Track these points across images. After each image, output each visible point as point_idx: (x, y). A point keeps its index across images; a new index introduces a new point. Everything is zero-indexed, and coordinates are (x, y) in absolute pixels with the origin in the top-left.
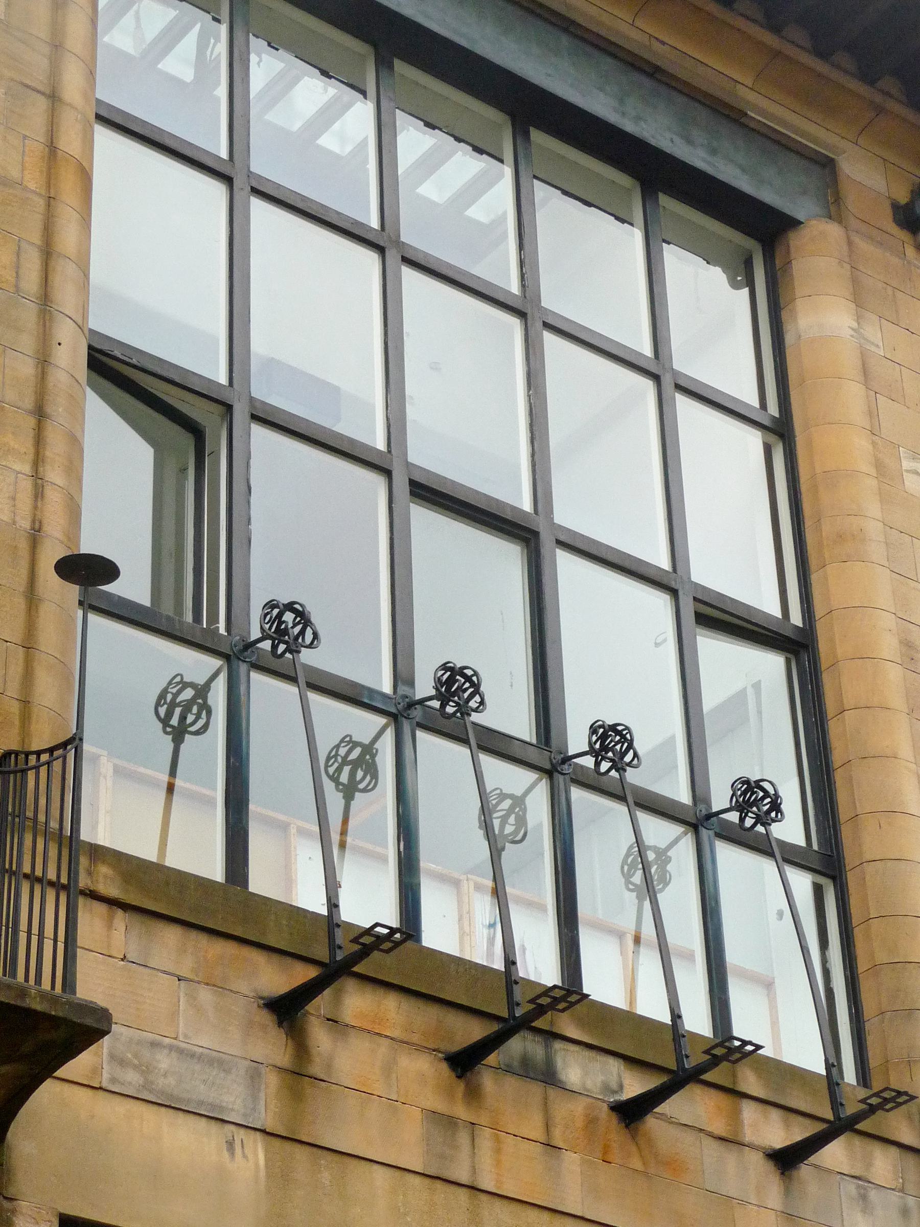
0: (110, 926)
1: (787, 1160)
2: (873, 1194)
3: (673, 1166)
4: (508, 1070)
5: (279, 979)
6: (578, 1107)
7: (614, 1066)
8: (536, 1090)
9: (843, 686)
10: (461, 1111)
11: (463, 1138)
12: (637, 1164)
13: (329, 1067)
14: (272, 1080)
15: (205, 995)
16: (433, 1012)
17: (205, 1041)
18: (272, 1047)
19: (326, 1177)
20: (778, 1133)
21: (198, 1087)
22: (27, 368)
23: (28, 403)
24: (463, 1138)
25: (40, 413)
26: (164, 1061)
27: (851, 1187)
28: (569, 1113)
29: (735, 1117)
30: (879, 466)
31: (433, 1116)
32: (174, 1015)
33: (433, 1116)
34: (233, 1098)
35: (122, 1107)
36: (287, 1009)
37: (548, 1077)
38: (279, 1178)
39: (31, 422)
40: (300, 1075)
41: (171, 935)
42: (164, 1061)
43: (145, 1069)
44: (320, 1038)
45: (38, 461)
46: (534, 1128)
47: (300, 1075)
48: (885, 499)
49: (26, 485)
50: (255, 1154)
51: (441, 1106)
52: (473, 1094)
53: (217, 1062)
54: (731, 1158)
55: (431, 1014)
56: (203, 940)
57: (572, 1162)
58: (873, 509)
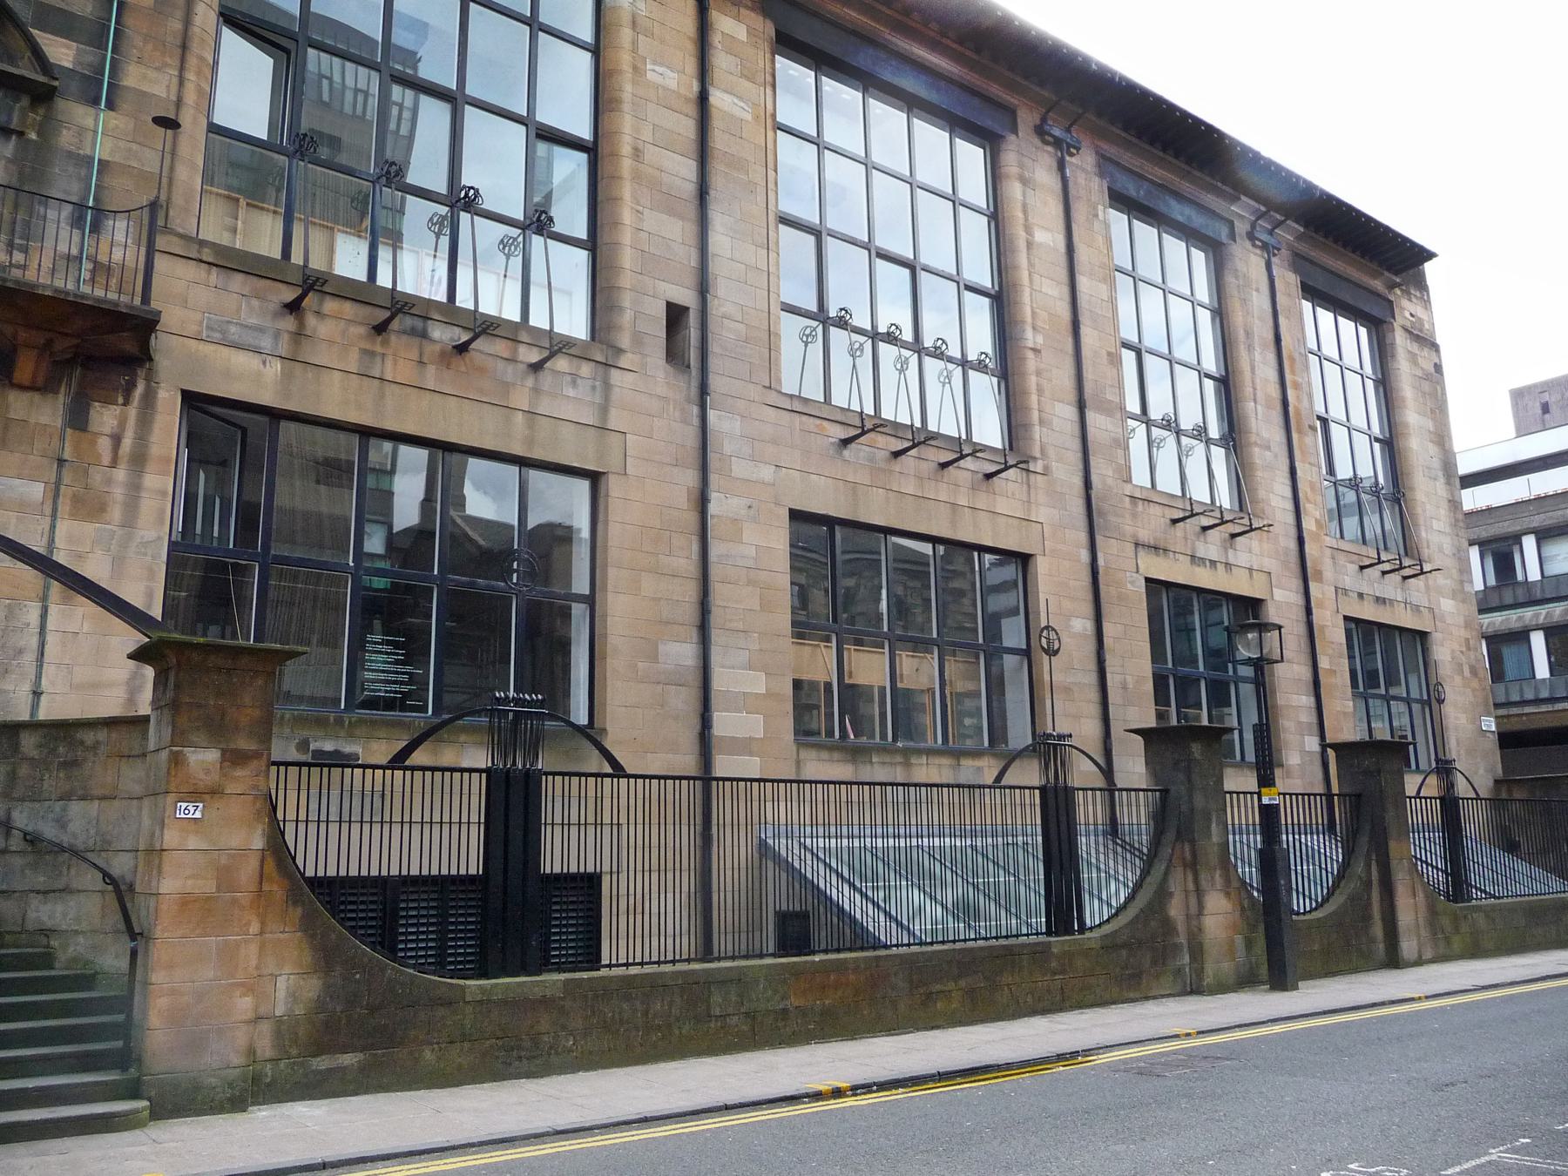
0: (209, 273)
1: (536, 367)
2: (579, 381)
3: (482, 370)
4: (404, 332)
5: (289, 295)
6: (437, 348)
7: (457, 330)
8: (417, 340)
9: (605, 168)
10: (379, 349)
11: (378, 359)
12: (463, 369)
13: (315, 330)
14: (286, 337)
15: (255, 303)
16: (369, 309)
17: (253, 321)
18: (289, 323)
19: (310, 375)
20: (534, 356)
21: (249, 338)
22: (176, 25)
23: (178, 42)
24: (378, 359)
25: (184, 47)
26: (233, 329)
27: (569, 378)
28: (430, 349)
29: (515, 351)
30: (635, 68)
31: (365, 352)
32: (239, 309)
33: (365, 352)
34: (266, 343)
35: (212, 347)
36: (294, 307)
37: (424, 335)
38: (287, 376)
39: (179, 51)
40: (299, 335)
41: (239, 277)
42: (233, 329)
43: (223, 332)
44: (311, 320)
45: (182, 69)
46: (415, 355)
47: (299, 335)
48: (634, 83)
49: (175, 81)
50: (277, 365)
51: (368, 346)
52: (385, 343)
53: (260, 330)
54: (510, 368)
55: (368, 310)
56: (255, 279)
57: (431, 370)
58: (628, 88)
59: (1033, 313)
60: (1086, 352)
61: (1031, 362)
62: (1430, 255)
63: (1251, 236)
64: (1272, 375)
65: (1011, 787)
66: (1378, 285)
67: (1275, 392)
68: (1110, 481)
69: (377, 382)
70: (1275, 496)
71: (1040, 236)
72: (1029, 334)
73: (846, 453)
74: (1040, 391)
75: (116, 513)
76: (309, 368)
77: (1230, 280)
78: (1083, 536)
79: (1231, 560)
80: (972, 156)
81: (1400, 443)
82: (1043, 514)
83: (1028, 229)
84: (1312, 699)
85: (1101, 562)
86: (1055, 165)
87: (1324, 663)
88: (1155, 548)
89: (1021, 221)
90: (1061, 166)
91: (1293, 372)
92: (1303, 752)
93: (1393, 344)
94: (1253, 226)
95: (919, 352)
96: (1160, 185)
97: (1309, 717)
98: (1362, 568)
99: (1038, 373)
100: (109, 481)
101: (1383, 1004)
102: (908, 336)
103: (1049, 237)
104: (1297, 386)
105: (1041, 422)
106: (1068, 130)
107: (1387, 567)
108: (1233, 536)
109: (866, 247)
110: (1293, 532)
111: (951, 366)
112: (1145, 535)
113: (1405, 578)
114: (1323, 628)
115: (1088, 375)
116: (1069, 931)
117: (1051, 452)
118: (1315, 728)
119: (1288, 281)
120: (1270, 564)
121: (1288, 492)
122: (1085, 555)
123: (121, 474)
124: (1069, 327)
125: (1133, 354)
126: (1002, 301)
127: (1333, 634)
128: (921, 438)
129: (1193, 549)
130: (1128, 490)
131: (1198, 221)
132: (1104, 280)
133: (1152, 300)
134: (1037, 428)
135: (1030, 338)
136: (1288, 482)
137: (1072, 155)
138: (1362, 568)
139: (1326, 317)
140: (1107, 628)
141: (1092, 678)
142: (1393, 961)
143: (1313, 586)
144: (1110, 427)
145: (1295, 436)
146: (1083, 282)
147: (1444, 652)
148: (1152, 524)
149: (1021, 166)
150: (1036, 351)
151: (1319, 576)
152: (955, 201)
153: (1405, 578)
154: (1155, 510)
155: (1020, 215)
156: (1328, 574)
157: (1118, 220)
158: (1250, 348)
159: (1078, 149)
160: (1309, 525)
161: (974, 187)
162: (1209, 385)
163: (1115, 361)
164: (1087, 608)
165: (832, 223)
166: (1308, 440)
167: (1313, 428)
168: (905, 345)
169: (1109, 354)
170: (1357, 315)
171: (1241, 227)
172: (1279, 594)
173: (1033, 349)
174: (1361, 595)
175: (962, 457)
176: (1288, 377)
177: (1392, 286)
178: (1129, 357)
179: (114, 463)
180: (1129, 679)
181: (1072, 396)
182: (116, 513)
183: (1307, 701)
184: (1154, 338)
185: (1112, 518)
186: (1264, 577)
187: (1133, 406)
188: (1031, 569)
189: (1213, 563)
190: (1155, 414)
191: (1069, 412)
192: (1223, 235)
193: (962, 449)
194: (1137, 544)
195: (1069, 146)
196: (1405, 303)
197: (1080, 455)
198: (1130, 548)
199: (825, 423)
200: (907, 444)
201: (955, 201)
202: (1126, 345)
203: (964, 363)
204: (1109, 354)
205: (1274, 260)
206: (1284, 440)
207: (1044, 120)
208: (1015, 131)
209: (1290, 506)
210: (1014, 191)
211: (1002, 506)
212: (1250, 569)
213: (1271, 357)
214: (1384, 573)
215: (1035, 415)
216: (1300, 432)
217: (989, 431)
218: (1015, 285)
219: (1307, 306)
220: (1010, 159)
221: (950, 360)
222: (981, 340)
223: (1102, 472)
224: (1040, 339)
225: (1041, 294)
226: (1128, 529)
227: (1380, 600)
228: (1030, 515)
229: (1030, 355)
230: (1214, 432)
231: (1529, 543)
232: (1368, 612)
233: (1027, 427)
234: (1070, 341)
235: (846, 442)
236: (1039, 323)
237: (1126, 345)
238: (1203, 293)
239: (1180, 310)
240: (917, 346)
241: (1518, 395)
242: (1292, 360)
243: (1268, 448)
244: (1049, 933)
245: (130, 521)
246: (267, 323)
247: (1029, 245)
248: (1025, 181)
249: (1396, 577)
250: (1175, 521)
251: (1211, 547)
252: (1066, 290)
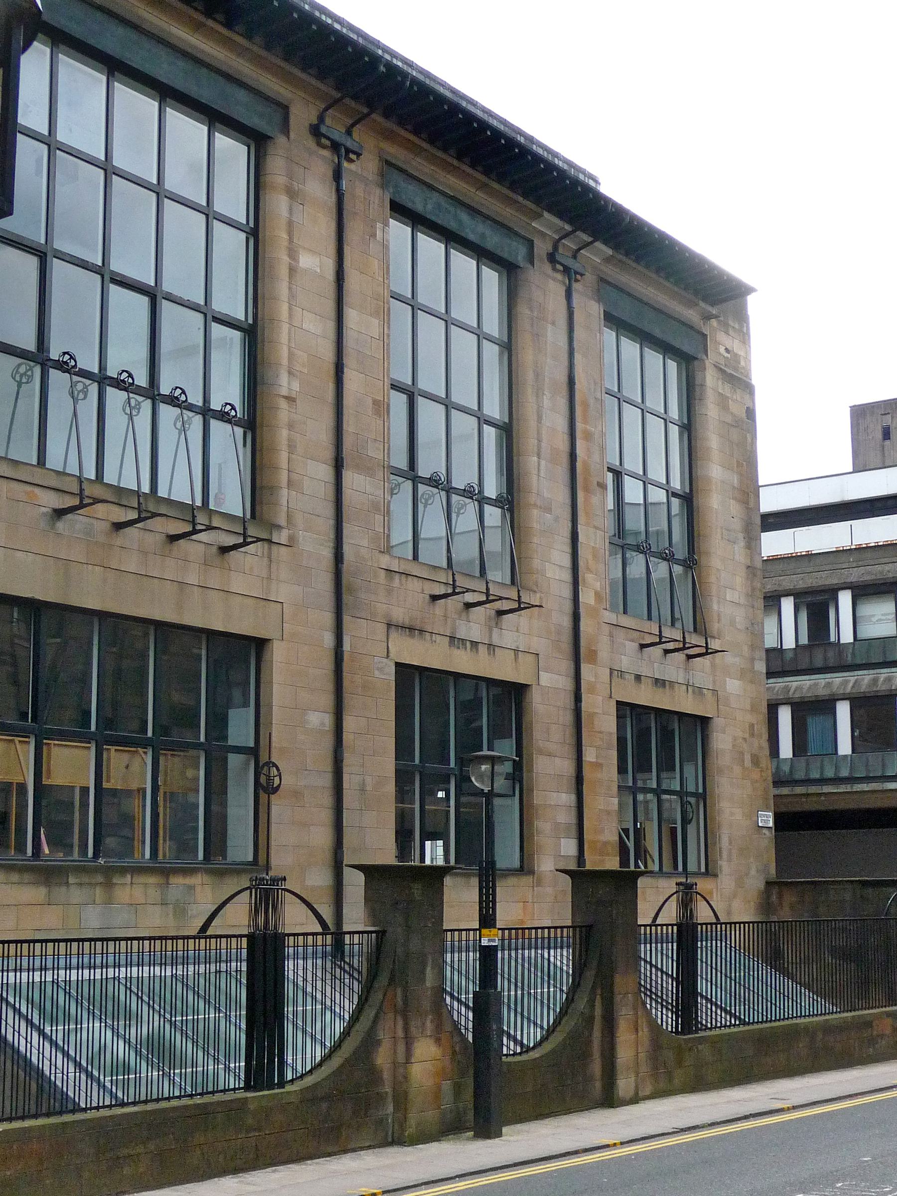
59: (291, 355)
60: (349, 400)
61: (284, 413)
62: (749, 290)
63: (552, 258)
64: (561, 423)
65: (216, 937)
66: (691, 315)
67: (562, 444)
68: (364, 552)
70: (551, 564)
71: (306, 261)
72: (284, 379)
73: (60, 525)
74: (292, 447)
77: (523, 310)
78: (328, 618)
79: (496, 641)
80: (233, 152)
81: (700, 501)
82: (284, 592)
83: (292, 254)
84: (573, 797)
85: (346, 647)
86: (330, 174)
87: (589, 755)
88: (411, 630)
89: (286, 244)
90: (337, 175)
91: (585, 421)
92: (558, 856)
93: (703, 385)
94: (555, 247)
95: (153, 399)
96: (452, 198)
97: (567, 818)
98: (643, 646)
99: (291, 426)
101: (576, 1153)
102: (142, 380)
103: (316, 263)
104: (588, 436)
105: (289, 482)
106: (349, 132)
107: (671, 646)
108: (500, 613)
109: (100, 271)
110: (568, 606)
111: (187, 414)
112: (399, 615)
113: (689, 657)
114: (592, 715)
115: (349, 426)
116: (271, 1086)
117: (299, 519)
118: (574, 831)
119: (589, 310)
120: (539, 644)
121: (567, 561)
122: (329, 639)
124: (332, 371)
125: (404, 397)
126: (253, 335)
127: (604, 723)
128: (146, 507)
129: (454, 629)
130: (385, 561)
131: (493, 240)
132: (375, 314)
133: (431, 330)
134: (285, 492)
135: (285, 383)
136: (568, 549)
137: (352, 161)
138: (643, 646)
139: (631, 348)
140: (349, 723)
141: (327, 780)
142: (609, 1100)
143: (585, 668)
144: (369, 489)
145: (580, 495)
146: (352, 316)
147: (723, 741)
148: (409, 599)
149: (290, 176)
150: (290, 399)
151: (593, 656)
152: (209, 214)
153: (689, 657)
154: (414, 585)
155: (285, 236)
156: (604, 654)
157: (399, 232)
158: (539, 392)
159: (358, 155)
160: (587, 598)
161: (233, 199)
162: (490, 433)
163: (382, 409)
164: (327, 700)
165: (60, 244)
166: (595, 500)
167: (602, 486)
168: (139, 391)
169: (375, 402)
170: (667, 349)
171: (542, 248)
172: (546, 679)
173: (286, 398)
174: (638, 678)
175: (195, 532)
176: (579, 426)
177: (707, 317)
178: (399, 401)
180: (368, 780)
181: (328, 453)
183: (569, 799)
184: (431, 380)
185: (362, 596)
186: (530, 658)
187: (402, 463)
188: (266, 657)
189: (474, 644)
190: (424, 471)
191: (324, 472)
192: (520, 257)
193: (194, 518)
194: (389, 625)
195: (348, 151)
196: (721, 336)
197: (332, 522)
198: (381, 628)
199: (37, 490)
200: (133, 515)
201: (209, 214)
202: (395, 387)
203: (206, 412)
204: (375, 402)
205: (575, 286)
206: (568, 501)
207: (321, 119)
208: (285, 129)
209: (567, 576)
210: (278, 205)
211: (238, 584)
212: (516, 651)
213: (562, 402)
214: (667, 652)
215: (284, 477)
216: (587, 490)
217: (231, 498)
218: (272, 320)
219: (610, 336)
220: (276, 165)
221: (190, 408)
222: (228, 390)
223: (356, 540)
224: (296, 386)
225: (301, 332)
226: (381, 608)
227: (659, 683)
228: (266, 596)
229: (283, 404)
230: (491, 490)
231: (845, 599)
232: (644, 696)
233: (273, 489)
234: (331, 387)
235: (59, 513)
236: (298, 367)
237: (395, 387)
238: (493, 325)
239: (464, 342)
240: (152, 392)
241: (860, 414)
242: (586, 405)
243: (548, 510)
244: (248, 1087)
247: (292, 270)
248: (292, 194)
249: (680, 657)
250: (434, 598)
251: (474, 627)
252: (331, 326)
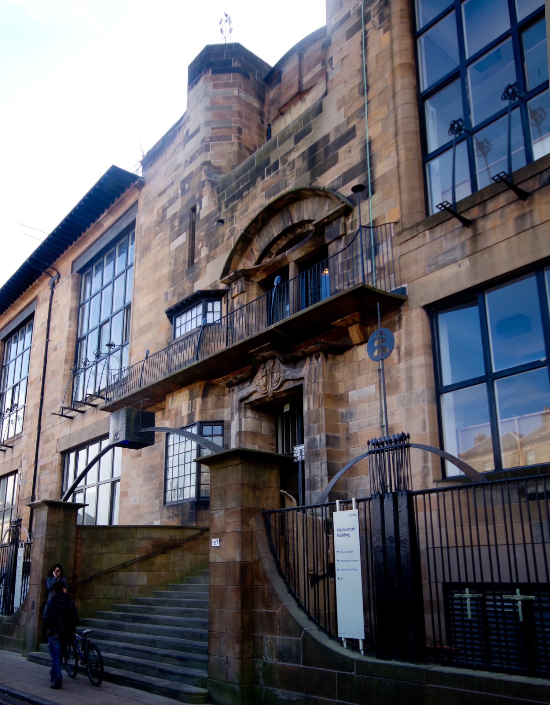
10: (527, 209)
19: (486, 256)
50: (466, 263)
69: (530, 231)
75: (403, 385)
76: (485, 251)
100: (398, 371)
123: (402, 365)
179: (399, 361)
182: (403, 385)
245: (410, 387)
246: (457, 242)
